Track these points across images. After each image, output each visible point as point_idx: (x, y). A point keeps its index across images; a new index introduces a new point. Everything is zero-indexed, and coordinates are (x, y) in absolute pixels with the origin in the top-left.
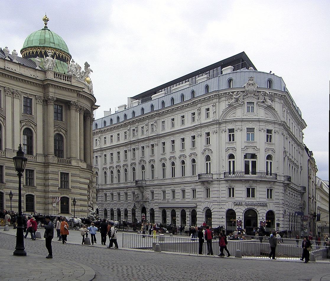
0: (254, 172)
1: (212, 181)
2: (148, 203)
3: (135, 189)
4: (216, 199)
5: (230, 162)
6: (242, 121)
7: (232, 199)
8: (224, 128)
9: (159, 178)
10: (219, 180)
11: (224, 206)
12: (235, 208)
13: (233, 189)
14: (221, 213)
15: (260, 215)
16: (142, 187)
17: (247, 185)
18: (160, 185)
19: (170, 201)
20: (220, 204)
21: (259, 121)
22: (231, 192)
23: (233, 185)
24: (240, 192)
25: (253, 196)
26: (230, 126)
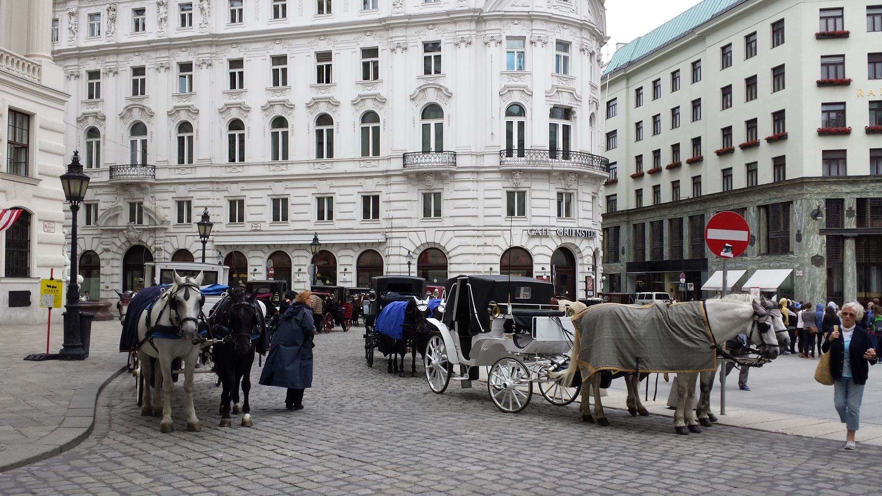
0: (567, 155)
1: (453, 173)
2: (162, 234)
3: (99, 191)
4: (468, 221)
5: (509, 124)
6: (548, 19)
7: (517, 221)
8: (495, 34)
9: (217, 161)
10: (477, 171)
11: (497, 241)
12: (530, 245)
13: (522, 195)
14: (488, 259)
15: (585, 261)
16: (139, 186)
17: (560, 186)
18: (217, 183)
19: (265, 227)
20: (480, 233)
21: (582, 26)
22: (516, 204)
23: (523, 184)
24: (542, 201)
25: (568, 214)
26: (517, 30)
